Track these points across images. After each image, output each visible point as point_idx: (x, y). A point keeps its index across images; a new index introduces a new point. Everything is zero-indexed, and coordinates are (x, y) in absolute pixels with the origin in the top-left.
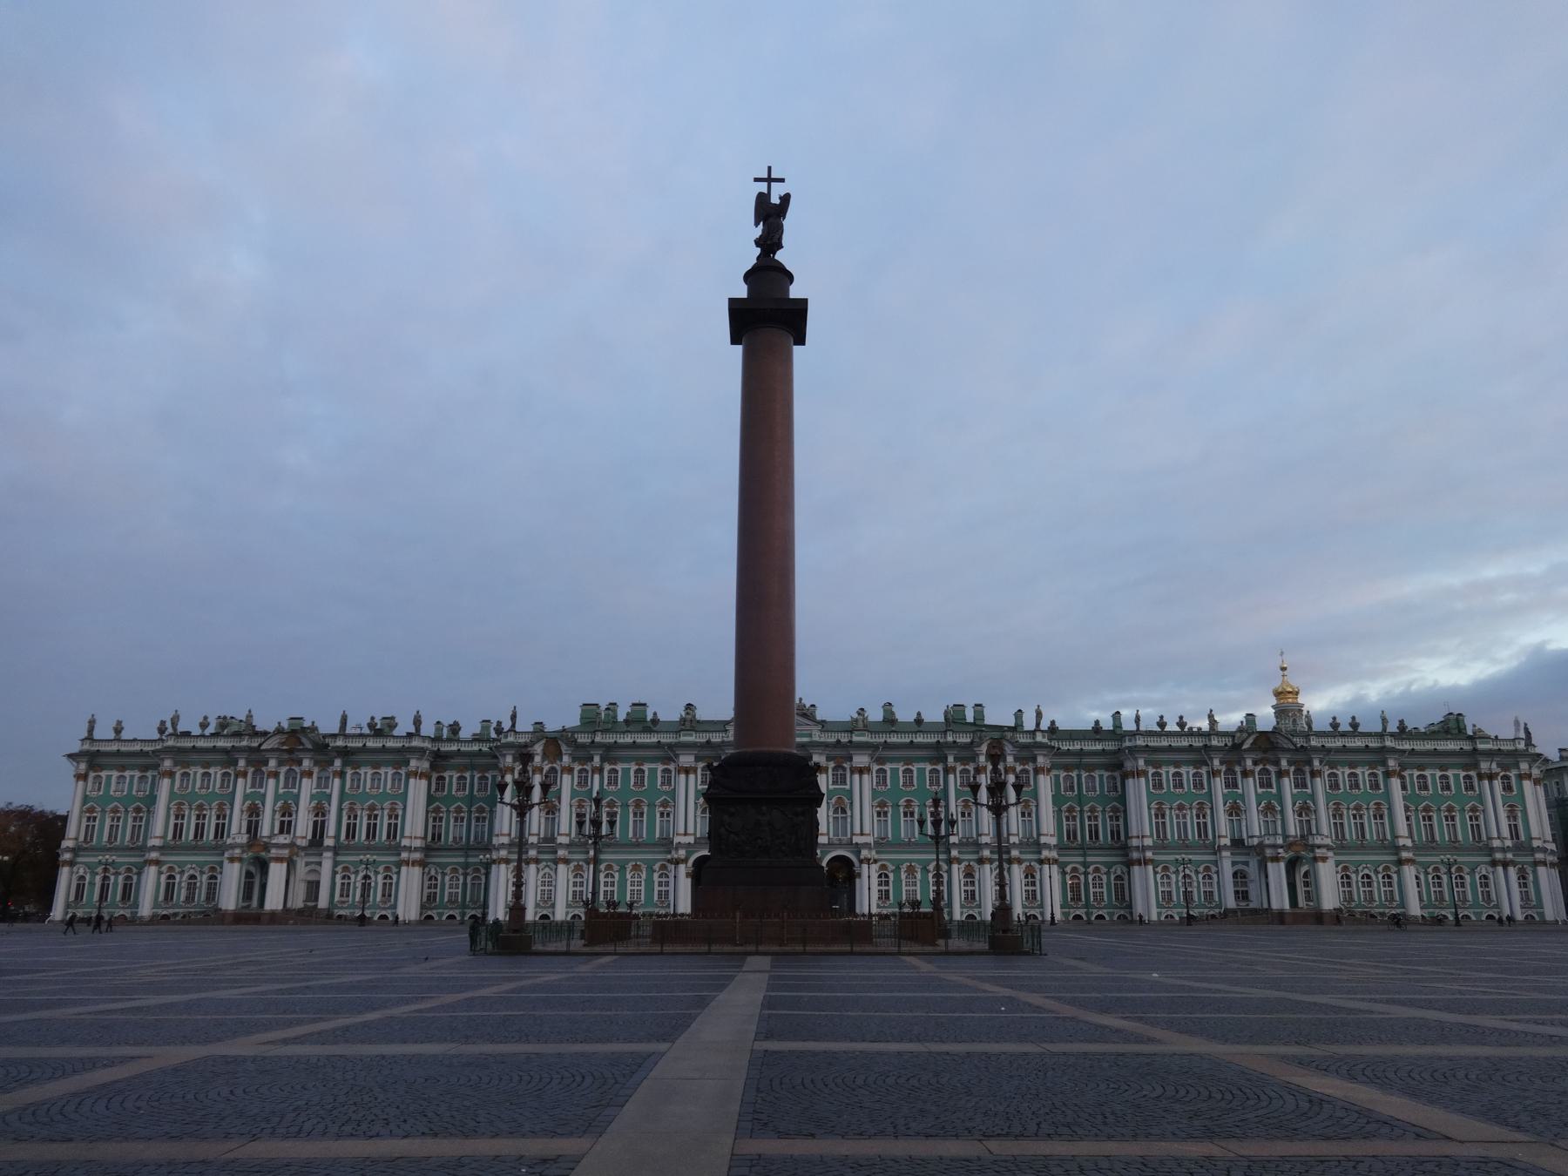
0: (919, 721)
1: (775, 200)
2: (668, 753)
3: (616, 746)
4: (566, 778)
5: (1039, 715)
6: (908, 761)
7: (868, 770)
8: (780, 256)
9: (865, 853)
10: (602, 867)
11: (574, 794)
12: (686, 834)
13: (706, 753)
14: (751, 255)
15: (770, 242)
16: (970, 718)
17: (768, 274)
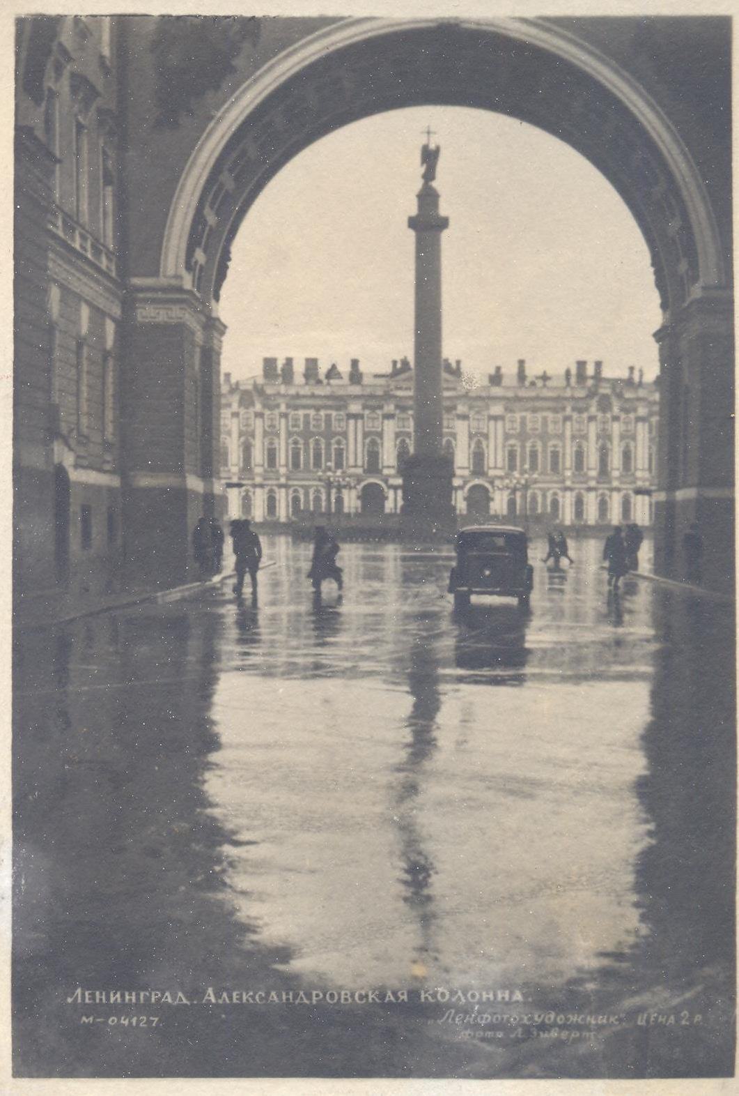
0: (545, 378)
1: (432, 146)
2: (339, 402)
3: (298, 396)
4: (259, 422)
5: (641, 376)
6: (535, 410)
7: (502, 418)
8: (434, 184)
9: (497, 483)
10: (291, 491)
11: (265, 434)
12: (356, 466)
13: (372, 403)
14: (418, 184)
15: (429, 175)
16: (590, 370)
17: (428, 197)
